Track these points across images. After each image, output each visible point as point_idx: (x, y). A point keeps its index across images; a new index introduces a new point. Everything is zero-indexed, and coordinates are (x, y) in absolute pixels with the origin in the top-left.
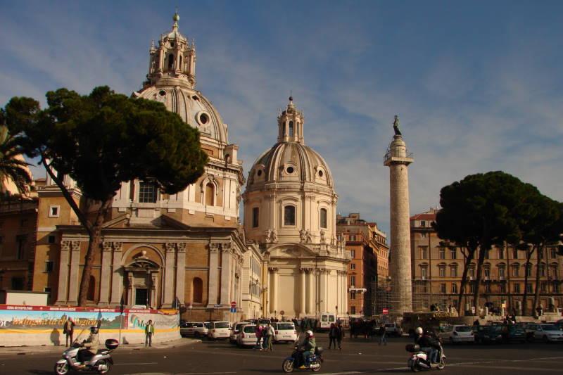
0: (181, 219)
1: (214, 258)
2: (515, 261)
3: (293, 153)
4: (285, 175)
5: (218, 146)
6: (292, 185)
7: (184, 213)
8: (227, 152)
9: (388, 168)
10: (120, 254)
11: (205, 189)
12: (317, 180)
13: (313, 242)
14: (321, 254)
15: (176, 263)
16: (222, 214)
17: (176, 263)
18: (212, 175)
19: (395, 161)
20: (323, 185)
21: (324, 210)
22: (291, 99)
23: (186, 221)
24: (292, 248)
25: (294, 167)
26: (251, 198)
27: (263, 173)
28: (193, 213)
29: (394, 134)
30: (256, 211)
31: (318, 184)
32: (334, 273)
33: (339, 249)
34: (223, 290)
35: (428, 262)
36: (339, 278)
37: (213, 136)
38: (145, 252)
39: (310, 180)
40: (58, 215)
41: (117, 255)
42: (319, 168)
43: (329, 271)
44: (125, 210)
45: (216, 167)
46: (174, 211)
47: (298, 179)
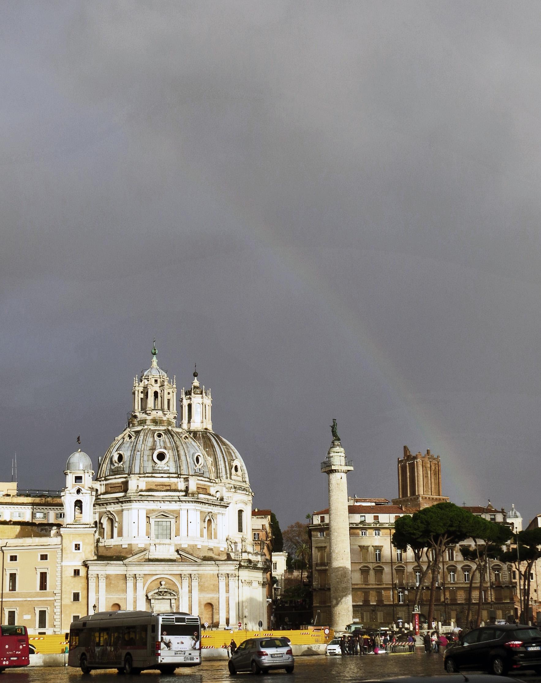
2: (452, 563)
10: (142, 584)
12: (233, 477)
15: (190, 592)
21: (240, 512)
22: (195, 375)
37: (205, 475)
38: (163, 583)
41: (140, 584)
46: (186, 546)
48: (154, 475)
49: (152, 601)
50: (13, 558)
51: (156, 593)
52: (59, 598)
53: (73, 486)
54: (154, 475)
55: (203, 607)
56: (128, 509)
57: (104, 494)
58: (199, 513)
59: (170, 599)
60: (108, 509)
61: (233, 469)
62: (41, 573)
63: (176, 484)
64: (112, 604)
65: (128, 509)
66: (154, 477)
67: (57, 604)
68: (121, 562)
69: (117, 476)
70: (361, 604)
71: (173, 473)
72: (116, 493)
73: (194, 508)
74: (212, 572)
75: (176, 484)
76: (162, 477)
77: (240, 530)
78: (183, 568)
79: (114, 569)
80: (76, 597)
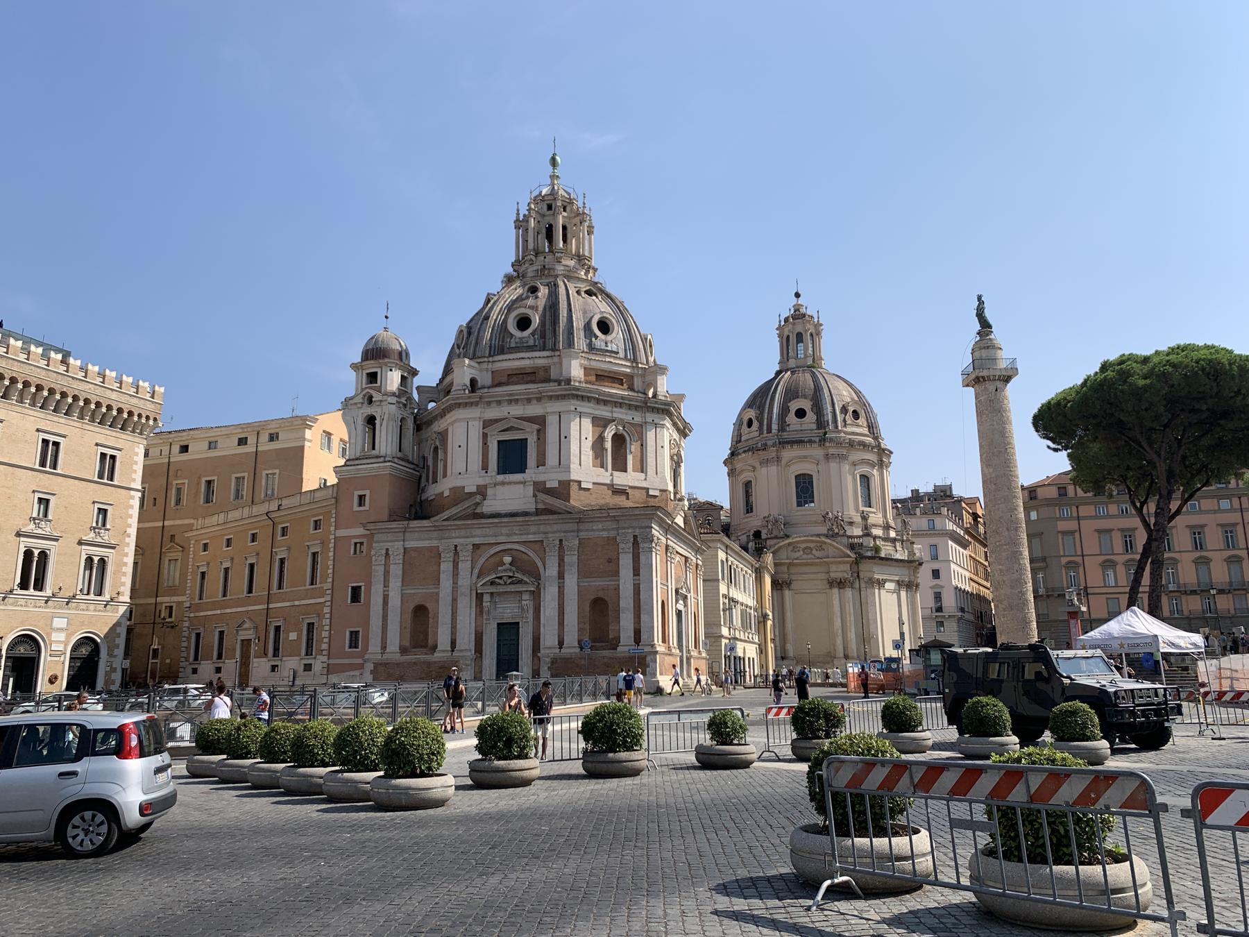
0: (567, 498)
1: (626, 561)
7: (574, 487)
9: (971, 390)
11: (608, 445)
13: (848, 533)
15: (561, 576)
16: (644, 485)
17: (561, 576)
23: (577, 500)
26: (739, 466)
27: (755, 424)
28: (590, 486)
30: (748, 485)
31: (853, 433)
32: (890, 586)
33: (898, 544)
34: (644, 617)
35: (1079, 559)
36: (903, 593)
39: (837, 427)
40: (367, 507)
41: (465, 566)
42: (851, 409)
43: (881, 584)
44: (474, 489)
45: (630, 407)
46: (556, 485)
47: (814, 426)
49: (486, 598)
51: (492, 583)
52: (329, 598)
55: (587, 605)
59: (521, 592)
63: (547, 369)
64: (412, 606)
67: (327, 610)
68: (425, 523)
74: (605, 534)
75: (547, 369)
78: (548, 528)
79: (420, 536)
80: (356, 593)
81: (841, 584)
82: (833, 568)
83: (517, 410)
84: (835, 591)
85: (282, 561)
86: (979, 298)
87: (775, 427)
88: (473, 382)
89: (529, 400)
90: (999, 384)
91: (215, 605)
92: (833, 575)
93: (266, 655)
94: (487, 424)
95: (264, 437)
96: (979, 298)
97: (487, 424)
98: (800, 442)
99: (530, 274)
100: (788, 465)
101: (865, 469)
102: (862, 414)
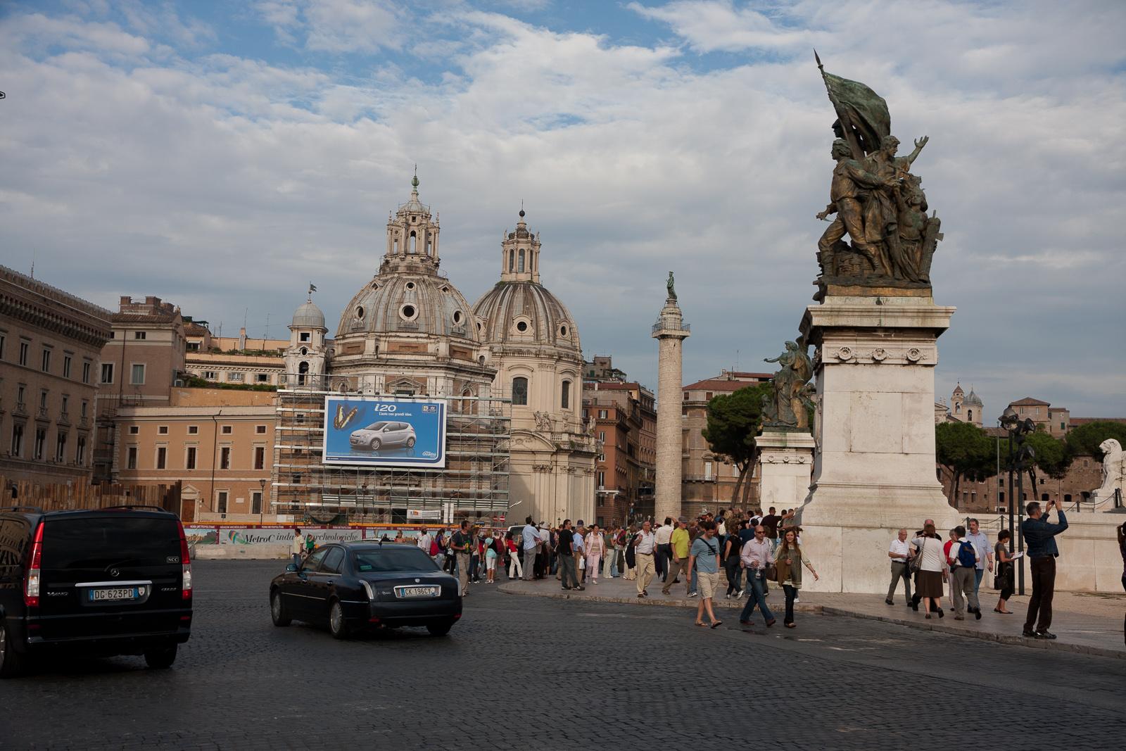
3: (526, 301)
4: (516, 333)
5: (470, 347)
6: (524, 347)
8: (481, 353)
12: (559, 342)
14: (562, 446)
18: (469, 382)
19: (667, 335)
20: (568, 348)
24: (522, 437)
25: (528, 322)
29: (667, 295)
31: (561, 347)
37: (466, 337)
47: (532, 339)
48: (398, 334)
50: (227, 430)
53: (299, 345)
54: (398, 334)
56: (364, 375)
57: (339, 356)
58: (451, 382)
60: (343, 375)
61: (559, 331)
62: (189, 448)
63: (425, 345)
65: (364, 375)
66: (398, 336)
69: (356, 335)
70: (730, 501)
71: (423, 333)
72: (353, 354)
73: (444, 375)
75: (425, 345)
76: (408, 337)
77: (565, 404)
81: (542, 469)
82: (538, 457)
83: (408, 373)
84: (538, 474)
85: (226, 451)
86: (671, 276)
87: (499, 336)
88: (377, 348)
89: (417, 367)
90: (677, 341)
91: (149, 474)
92: (537, 463)
93: (211, 510)
94: (388, 378)
95: (131, 335)
96: (671, 274)
97: (388, 378)
98: (520, 352)
99: (401, 269)
100: (510, 369)
101: (567, 376)
102: (567, 332)
